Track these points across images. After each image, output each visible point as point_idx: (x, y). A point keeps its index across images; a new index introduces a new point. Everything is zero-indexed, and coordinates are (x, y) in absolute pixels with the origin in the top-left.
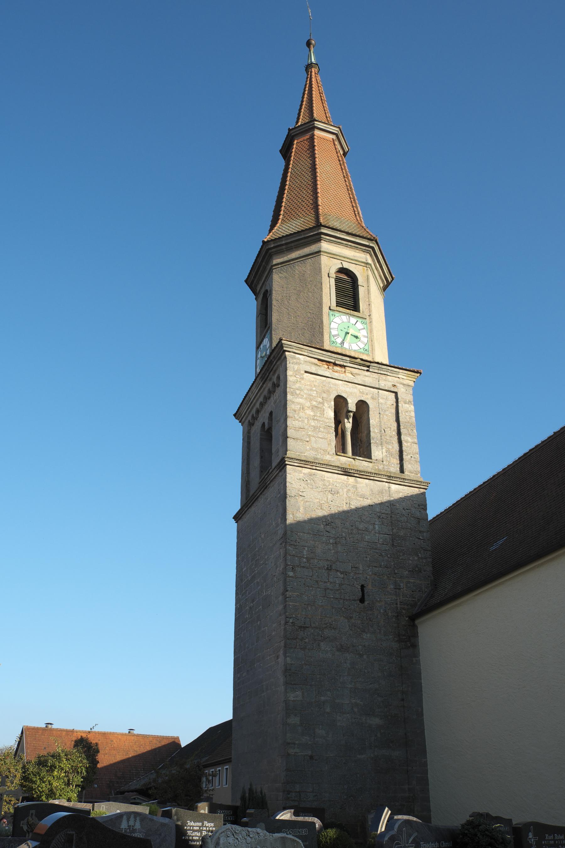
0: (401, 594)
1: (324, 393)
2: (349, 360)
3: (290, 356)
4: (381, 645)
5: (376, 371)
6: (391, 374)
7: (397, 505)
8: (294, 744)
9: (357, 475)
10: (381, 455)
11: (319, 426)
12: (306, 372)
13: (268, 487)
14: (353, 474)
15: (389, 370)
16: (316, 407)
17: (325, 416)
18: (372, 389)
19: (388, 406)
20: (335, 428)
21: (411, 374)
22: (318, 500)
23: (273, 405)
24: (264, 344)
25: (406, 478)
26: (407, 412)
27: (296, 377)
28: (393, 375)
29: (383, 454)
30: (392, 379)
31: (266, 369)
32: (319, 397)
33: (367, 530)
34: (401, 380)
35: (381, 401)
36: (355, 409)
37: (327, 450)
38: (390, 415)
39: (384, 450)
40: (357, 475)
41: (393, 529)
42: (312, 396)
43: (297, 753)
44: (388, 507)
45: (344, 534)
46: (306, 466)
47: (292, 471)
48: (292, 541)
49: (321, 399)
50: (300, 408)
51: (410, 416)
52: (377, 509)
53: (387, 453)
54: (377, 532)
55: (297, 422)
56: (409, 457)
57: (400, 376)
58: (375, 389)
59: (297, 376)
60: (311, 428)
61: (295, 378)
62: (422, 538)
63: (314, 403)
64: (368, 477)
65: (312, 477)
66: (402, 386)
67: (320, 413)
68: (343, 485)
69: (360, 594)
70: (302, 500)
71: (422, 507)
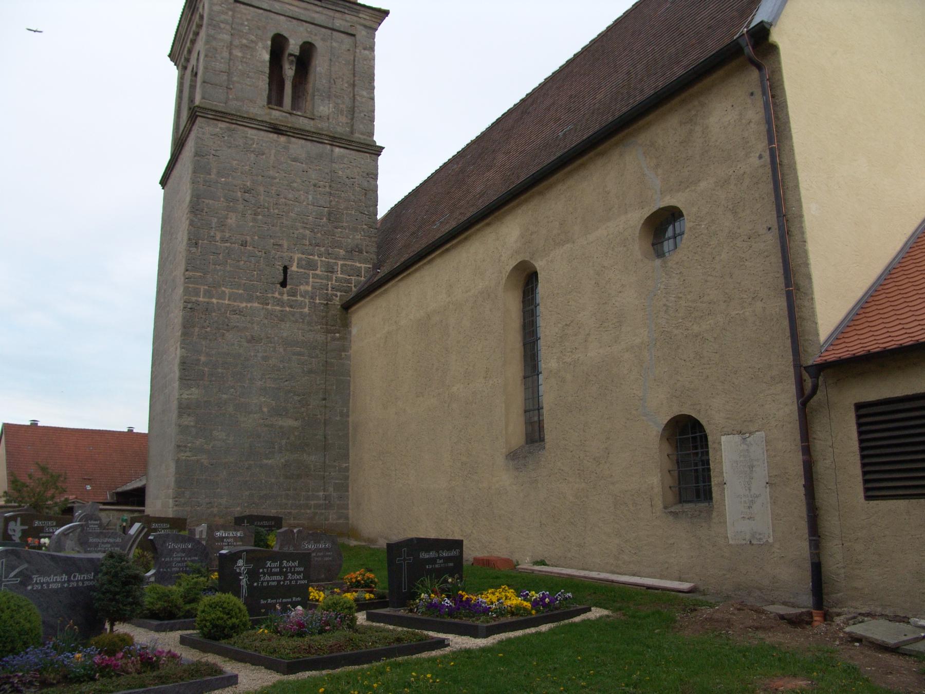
0: (334, 278)
1: (259, 29)
4: (303, 336)
8: (185, 446)
9: (291, 134)
14: (285, 133)
16: (247, 46)
18: (324, 30)
22: (236, 162)
25: (354, 140)
29: (329, 110)
30: (351, 19)
33: (296, 200)
34: (362, 21)
35: (334, 44)
36: (298, 52)
39: (331, 105)
40: (291, 134)
41: (331, 201)
42: (243, 32)
43: (189, 457)
44: (327, 174)
45: (266, 204)
46: (223, 119)
48: (197, 210)
49: (253, 37)
50: (224, 46)
54: (310, 203)
56: (362, 115)
57: (361, 15)
59: (223, 5)
61: (220, 8)
62: (367, 213)
63: (244, 41)
64: (305, 137)
66: (362, 28)
69: (281, 278)
70: (215, 161)
71: (372, 176)
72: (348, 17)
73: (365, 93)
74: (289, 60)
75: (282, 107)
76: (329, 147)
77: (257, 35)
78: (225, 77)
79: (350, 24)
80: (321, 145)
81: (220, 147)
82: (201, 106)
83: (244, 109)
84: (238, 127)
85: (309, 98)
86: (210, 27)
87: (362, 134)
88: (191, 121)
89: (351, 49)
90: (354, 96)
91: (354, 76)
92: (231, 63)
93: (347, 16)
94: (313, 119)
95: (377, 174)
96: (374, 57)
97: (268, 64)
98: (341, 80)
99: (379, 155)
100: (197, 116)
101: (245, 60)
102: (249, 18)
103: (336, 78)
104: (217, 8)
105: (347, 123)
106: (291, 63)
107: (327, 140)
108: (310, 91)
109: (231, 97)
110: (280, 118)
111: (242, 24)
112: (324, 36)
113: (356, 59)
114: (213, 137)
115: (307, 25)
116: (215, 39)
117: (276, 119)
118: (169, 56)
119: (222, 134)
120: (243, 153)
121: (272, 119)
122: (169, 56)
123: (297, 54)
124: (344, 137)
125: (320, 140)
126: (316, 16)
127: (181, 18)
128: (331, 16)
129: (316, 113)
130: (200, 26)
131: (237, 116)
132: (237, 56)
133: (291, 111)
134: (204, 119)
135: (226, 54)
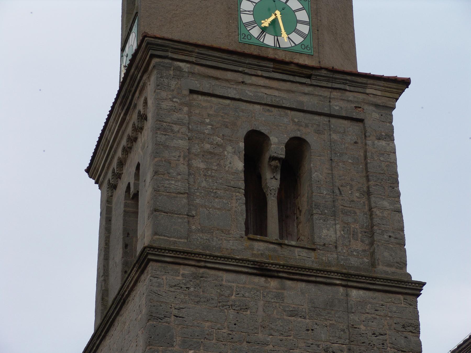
2: (272, 66)
3: (162, 64)
5: (324, 84)
6: (352, 89)
7: (362, 327)
10: (333, 236)
11: (215, 187)
12: (192, 92)
13: (127, 301)
14: (276, 274)
15: (346, 80)
16: (211, 153)
17: (227, 168)
18: (316, 117)
19: (347, 145)
20: (245, 190)
21: (389, 86)
22: (208, 324)
23: (141, 152)
24: (130, 45)
25: (378, 275)
26: (383, 154)
27: (173, 101)
28: (356, 89)
30: (355, 97)
31: (126, 90)
32: (217, 135)
34: (371, 99)
36: (284, 153)
37: (229, 230)
38: (350, 161)
39: (338, 226)
42: (204, 133)
44: (343, 330)
46: (186, 262)
47: (161, 271)
49: (220, 139)
50: (179, 156)
51: (388, 161)
52: (323, 335)
53: (343, 230)
55: (173, 182)
57: (368, 91)
58: (322, 117)
59: (174, 100)
60: (201, 193)
61: (171, 104)
63: (207, 146)
65: (198, 282)
66: (373, 108)
67: (218, 164)
68: (258, 293)
71: (411, 328)
72: (350, 96)
73: (386, 204)
74: (270, 166)
75: (266, 236)
76: (341, 289)
77: (223, 135)
78: (185, 201)
79: (353, 105)
80: (330, 288)
81: (185, 303)
82: (155, 245)
83: (214, 244)
84: (207, 271)
85: (303, 218)
86: (159, 132)
87: (389, 265)
88: (139, 267)
89: (359, 141)
90: (370, 209)
91: (368, 180)
92: (191, 180)
93: (348, 93)
94: (314, 250)
95: (419, 325)
96: (395, 149)
97: (242, 175)
98: (348, 187)
99: (419, 295)
100: (150, 260)
101: (209, 172)
102: (211, 113)
103: (342, 186)
104: (165, 105)
105: (364, 251)
106: (274, 170)
107: (339, 279)
108: (304, 207)
109: (194, 227)
110: (267, 253)
111: (203, 123)
112: (319, 125)
113: (369, 154)
114: (172, 289)
115: (293, 113)
116: (167, 147)
117: (262, 254)
118: (88, 171)
119: (185, 284)
120: (217, 309)
121: (253, 255)
122: (88, 171)
123: (283, 156)
124: (363, 273)
125: (328, 281)
126: (305, 99)
127: (108, 119)
128: (325, 97)
129: (317, 240)
130: (138, 129)
131: (206, 255)
132: (198, 168)
133: (281, 241)
134: (159, 264)
135: (183, 168)
